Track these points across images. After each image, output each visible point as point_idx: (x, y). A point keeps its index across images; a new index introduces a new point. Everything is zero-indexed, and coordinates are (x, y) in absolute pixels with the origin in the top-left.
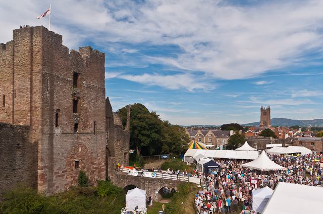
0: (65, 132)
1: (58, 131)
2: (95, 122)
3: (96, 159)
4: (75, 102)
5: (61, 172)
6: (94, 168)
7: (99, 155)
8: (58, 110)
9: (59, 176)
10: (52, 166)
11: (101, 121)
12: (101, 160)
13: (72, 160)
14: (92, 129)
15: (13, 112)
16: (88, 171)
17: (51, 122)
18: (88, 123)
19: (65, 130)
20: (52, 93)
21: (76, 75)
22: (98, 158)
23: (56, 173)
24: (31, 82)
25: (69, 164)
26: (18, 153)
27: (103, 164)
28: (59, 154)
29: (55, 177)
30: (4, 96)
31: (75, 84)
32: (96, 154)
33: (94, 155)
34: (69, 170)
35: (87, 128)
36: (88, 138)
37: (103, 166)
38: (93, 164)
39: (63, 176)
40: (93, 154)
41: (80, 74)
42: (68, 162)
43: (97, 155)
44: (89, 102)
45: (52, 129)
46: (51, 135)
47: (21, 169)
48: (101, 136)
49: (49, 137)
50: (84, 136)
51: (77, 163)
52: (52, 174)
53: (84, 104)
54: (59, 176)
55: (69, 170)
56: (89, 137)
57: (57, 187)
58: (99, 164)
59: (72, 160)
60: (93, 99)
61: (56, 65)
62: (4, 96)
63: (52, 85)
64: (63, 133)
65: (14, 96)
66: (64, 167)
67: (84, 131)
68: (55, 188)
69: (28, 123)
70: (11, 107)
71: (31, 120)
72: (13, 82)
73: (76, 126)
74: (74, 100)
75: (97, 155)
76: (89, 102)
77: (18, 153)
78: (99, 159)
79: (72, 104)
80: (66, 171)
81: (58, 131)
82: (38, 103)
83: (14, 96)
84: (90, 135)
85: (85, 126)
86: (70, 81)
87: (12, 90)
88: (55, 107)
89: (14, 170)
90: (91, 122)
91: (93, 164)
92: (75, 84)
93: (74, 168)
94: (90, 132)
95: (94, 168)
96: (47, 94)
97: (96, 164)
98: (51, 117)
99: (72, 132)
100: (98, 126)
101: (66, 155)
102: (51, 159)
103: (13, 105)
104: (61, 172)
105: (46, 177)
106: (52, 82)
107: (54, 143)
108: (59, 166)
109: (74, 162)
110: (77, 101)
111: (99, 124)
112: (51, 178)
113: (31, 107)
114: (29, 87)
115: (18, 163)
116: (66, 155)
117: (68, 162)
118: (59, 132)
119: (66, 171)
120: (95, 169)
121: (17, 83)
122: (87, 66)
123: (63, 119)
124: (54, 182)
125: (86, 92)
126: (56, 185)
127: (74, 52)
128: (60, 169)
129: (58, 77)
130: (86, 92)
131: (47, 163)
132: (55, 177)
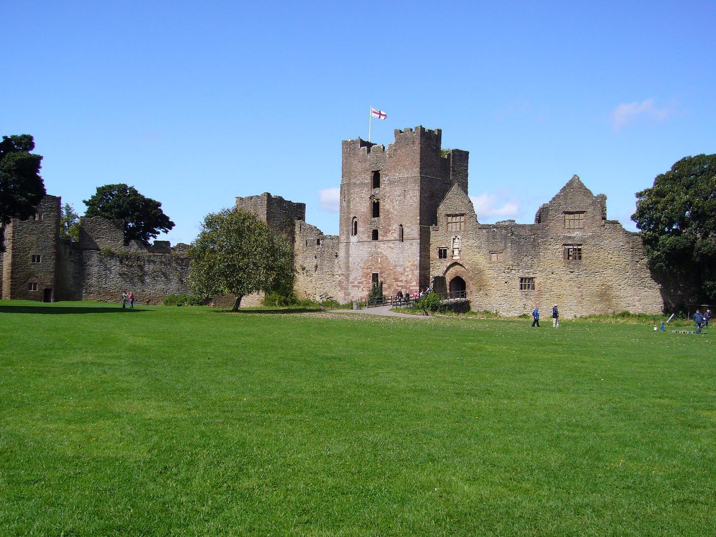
1: (354, 239)
3: (402, 274)
5: (356, 283)
6: (398, 286)
7: (407, 269)
9: (354, 286)
10: (348, 274)
11: (411, 223)
12: (410, 276)
14: (396, 235)
16: (390, 288)
17: (347, 231)
18: (390, 228)
19: (361, 239)
20: (349, 202)
22: (406, 274)
23: (352, 283)
27: (414, 283)
28: (355, 263)
29: (350, 286)
31: (376, 182)
32: (402, 268)
33: (399, 269)
34: (365, 282)
35: (389, 234)
36: (390, 247)
37: (413, 286)
38: (396, 280)
39: (359, 287)
41: (379, 171)
42: (364, 273)
43: (404, 269)
44: (392, 201)
45: (348, 238)
46: (348, 243)
48: (411, 244)
49: (346, 246)
52: (348, 283)
53: (385, 206)
54: (354, 286)
55: (365, 282)
56: (392, 245)
57: (353, 297)
59: (369, 270)
60: (399, 196)
61: (354, 172)
66: (360, 278)
67: (385, 238)
68: (350, 297)
75: (404, 269)
76: (392, 201)
78: (408, 275)
80: (362, 283)
85: (386, 232)
88: (352, 216)
89: (333, 275)
90: (395, 226)
91: (396, 280)
92: (376, 182)
93: (371, 281)
94: (393, 238)
95: (398, 286)
96: (345, 204)
97: (401, 281)
100: (406, 230)
101: (362, 265)
102: (348, 268)
104: (356, 283)
105: (342, 284)
106: (348, 191)
107: (350, 252)
108: (354, 276)
110: (378, 203)
112: (346, 287)
116: (362, 265)
117: (364, 273)
118: (355, 241)
119: (362, 283)
122: (390, 157)
124: (350, 291)
125: (388, 190)
128: (355, 279)
129: (355, 184)
130: (388, 190)
131: (343, 271)
132: (350, 286)
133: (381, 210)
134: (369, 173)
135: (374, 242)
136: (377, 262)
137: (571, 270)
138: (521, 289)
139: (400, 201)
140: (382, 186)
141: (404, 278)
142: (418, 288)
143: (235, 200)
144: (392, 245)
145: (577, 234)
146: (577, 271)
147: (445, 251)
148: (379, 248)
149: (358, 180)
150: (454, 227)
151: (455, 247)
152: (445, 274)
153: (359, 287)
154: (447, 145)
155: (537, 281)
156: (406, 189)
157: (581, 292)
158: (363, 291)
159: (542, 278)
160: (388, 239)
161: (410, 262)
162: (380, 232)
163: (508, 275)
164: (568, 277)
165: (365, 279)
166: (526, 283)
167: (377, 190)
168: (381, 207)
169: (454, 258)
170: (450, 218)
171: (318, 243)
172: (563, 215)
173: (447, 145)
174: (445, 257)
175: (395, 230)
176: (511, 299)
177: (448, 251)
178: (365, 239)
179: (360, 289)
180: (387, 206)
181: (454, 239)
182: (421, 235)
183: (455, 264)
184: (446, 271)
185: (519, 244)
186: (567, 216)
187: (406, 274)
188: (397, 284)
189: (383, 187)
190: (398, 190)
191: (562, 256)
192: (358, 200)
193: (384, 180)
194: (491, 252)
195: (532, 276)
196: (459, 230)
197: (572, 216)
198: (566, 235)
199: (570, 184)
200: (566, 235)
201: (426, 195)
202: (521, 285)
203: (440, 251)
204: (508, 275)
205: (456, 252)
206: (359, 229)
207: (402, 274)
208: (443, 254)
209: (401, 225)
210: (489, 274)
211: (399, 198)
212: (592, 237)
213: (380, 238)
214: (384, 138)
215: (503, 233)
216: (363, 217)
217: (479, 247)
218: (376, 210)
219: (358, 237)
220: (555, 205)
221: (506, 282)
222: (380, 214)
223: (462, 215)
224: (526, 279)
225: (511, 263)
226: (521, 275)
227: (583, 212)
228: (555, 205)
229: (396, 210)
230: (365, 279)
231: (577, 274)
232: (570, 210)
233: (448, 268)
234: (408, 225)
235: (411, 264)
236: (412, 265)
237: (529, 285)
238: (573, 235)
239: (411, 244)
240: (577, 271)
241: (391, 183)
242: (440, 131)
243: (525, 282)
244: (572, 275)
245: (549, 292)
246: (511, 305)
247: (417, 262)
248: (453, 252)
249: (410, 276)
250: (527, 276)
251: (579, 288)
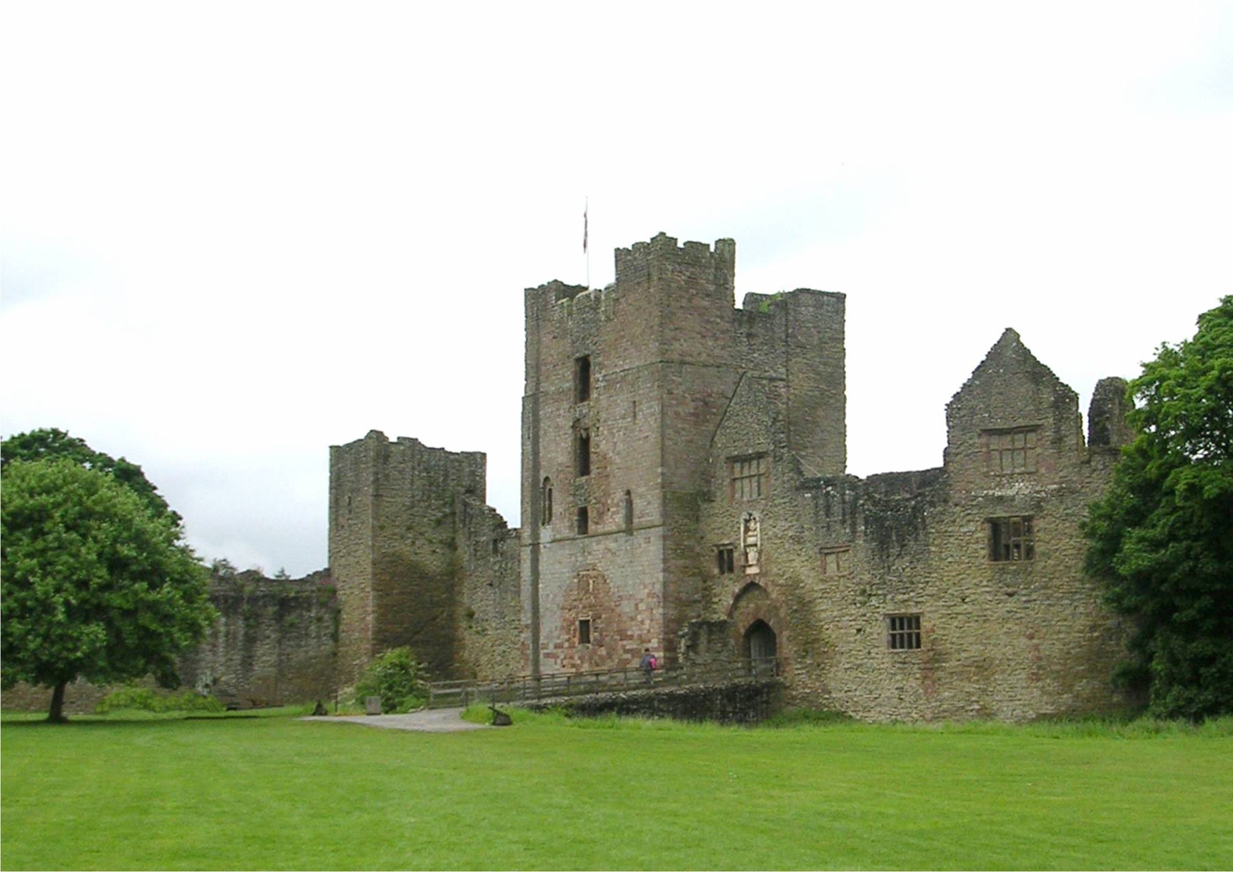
0: (558, 537)
2: (628, 493)
3: (632, 619)
4: (583, 447)
7: (642, 607)
8: (547, 479)
12: (647, 622)
19: (559, 532)
22: (639, 618)
27: (654, 643)
31: (583, 389)
33: (627, 607)
35: (607, 517)
36: (610, 550)
38: (624, 636)
40: (625, 602)
45: (535, 535)
46: (535, 547)
48: (648, 540)
50: (598, 543)
51: (585, 624)
53: (601, 444)
56: (612, 545)
58: (642, 640)
64: (553, 542)
73: (583, 513)
78: (642, 622)
81: (546, 534)
84: (616, 541)
88: (543, 475)
90: (619, 495)
93: (576, 640)
94: (614, 528)
97: (631, 637)
99: (571, 535)
100: (638, 503)
104: (551, 646)
109: (577, 623)
110: (588, 438)
111: (641, 496)
120: (629, 656)
122: (608, 319)
133: (593, 457)
134: (571, 363)
137: (1010, 590)
138: (894, 646)
139: (626, 428)
140: (594, 395)
141: (634, 631)
142: (661, 654)
143: (328, 450)
144: (612, 545)
145: (1020, 489)
146: (1024, 592)
147: (730, 551)
148: (590, 554)
149: (552, 384)
150: (747, 489)
151: (751, 540)
152: (730, 615)
153: (555, 657)
154: (752, 278)
155: (925, 624)
156: (637, 399)
157: (1036, 647)
159: (937, 615)
160: (607, 529)
161: (645, 587)
162: (592, 514)
163: (862, 611)
164: (1002, 610)
166: (905, 632)
167: (583, 408)
168: (592, 444)
169: (750, 571)
170: (738, 466)
171: (496, 551)
172: (984, 440)
173: (752, 278)
174: (731, 569)
175: (617, 505)
176: (872, 676)
177: (736, 554)
178: (566, 533)
180: (603, 446)
181: (747, 521)
182: (665, 515)
183: (751, 586)
184: (735, 606)
185: (882, 525)
186: (996, 443)
187: (639, 618)
188: (624, 646)
189: (595, 395)
190: (622, 403)
191: (983, 552)
193: (597, 376)
194: (824, 552)
195: (915, 610)
196: (755, 496)
197: (1006, 441)
198: (991, 492)
199: (995, 354)
200: (991, 492)
201: (680, 409)
202: (894, 636)
203: (721, 552)
204: (862, 611)
205: (752, 555)
206: (557, 509)
207: (632, 619)
208: (726, 560)
209: (628, 493)
210: (825, 610)
211: (621, 423)
212: (1060, 494)
213: (592, 527)
214: (598, 274)
215: (847, 498)
216: (561, 476)
217: (798, 540)
220: (962, 413)
221: (859, 631)
223: (760, 456)
224: (901, 619)
225: (867, 577)
226: (890, 608)
227: (1034, 429)
228: (962, 413)
231: (1024, 599)
232: (1000, 424)
233: (738, 598)
234: (642, 490)
235: (647, 591)
236: (649, 594)
237: (910, 635)
238: (1010, 493)
239: (648, 540)
240: (1024, 592)
241: (610, 383)
242: (727, 247)
243: (902, 628)
244: (1011, 604)
245: (958, 651)
246: (871, 692)
247: (658, 588)
248: (746, 554)
249: (647, 622)
250: (903, 611)
251: (1031, 637)
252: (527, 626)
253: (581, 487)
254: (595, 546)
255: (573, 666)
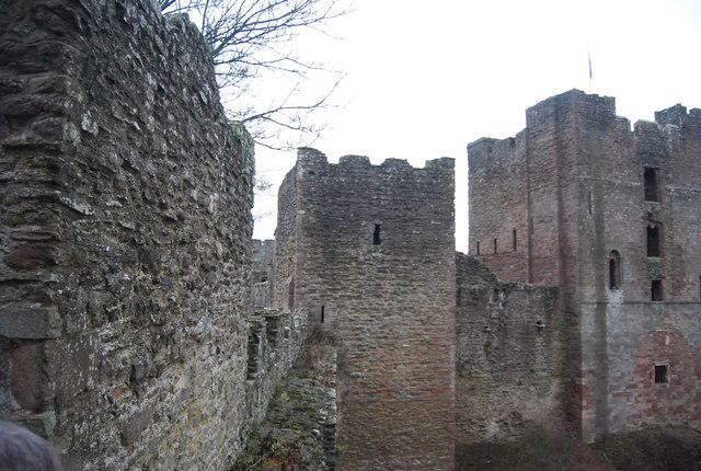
1: (615, 298)
9: (619, 395)
13: (647, 361)
15: (530, 260)
17: (599, 278)
21: (650, 175)
24: (560, 199)
25: (642, 370)
26: (539, 340)
29: (610, 396)
30: (515, 232)
35: (684, 291)
39: (628, 396)
41: (658, 169)
46: (602, 305)
47: (544, 370)
49: (597, 309)
50: (675, 309)
53: (672, 236)
56: (689, 312)
62: (515, 232)
63: (599, 203)
65: (531, 230)
67: (677, 299)
69: (556, 282)
70: (526, 250)
71: (563, 273)
72: (530, 203)
74: (649, 228)
77: (539, 340)
79: (645, 237)
80: (634, 386)
82: (587, 327)
83: (531, 230)
85: (678, 287)
86: (638, 188)
87: (526, 218)
88: (609, 248)
89: (532, 371)
93: (653, 381)
94: (690, 300)
98: (599, 267)
102: (602, 357)
103: (530, 246)
107: (608, 323)
113: (561, 249)
114: (556, 210)
115: (540, 358)
119: (634, 386)
121: (537, 205)
123: (629, 273)
124: (609, 406)
126: (613, 414)
127: (641, 125)
135: (657, 306)
136: (663, 344)
153: (628, 396)
158: (637, 402)
162: (666, 286)
165: (642, 379)
175: (692, 284)
178: (640, 298)
179: (632, 399)
192: (619, 217)
213: (668, 297)
218: (654, 239)
219: (625, 293)
222: (666, 252)
229: (692, 247)
230: (642, 379)
241: (682, 197)
252: (591, 372)
253: (654, 264)
254: (671, 311)
255: (649, 401)
